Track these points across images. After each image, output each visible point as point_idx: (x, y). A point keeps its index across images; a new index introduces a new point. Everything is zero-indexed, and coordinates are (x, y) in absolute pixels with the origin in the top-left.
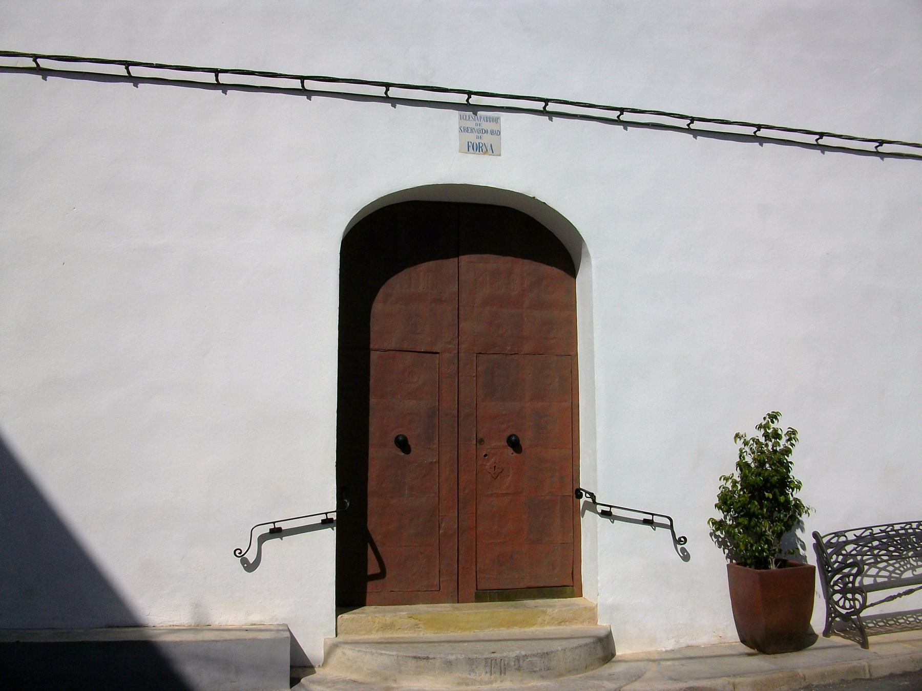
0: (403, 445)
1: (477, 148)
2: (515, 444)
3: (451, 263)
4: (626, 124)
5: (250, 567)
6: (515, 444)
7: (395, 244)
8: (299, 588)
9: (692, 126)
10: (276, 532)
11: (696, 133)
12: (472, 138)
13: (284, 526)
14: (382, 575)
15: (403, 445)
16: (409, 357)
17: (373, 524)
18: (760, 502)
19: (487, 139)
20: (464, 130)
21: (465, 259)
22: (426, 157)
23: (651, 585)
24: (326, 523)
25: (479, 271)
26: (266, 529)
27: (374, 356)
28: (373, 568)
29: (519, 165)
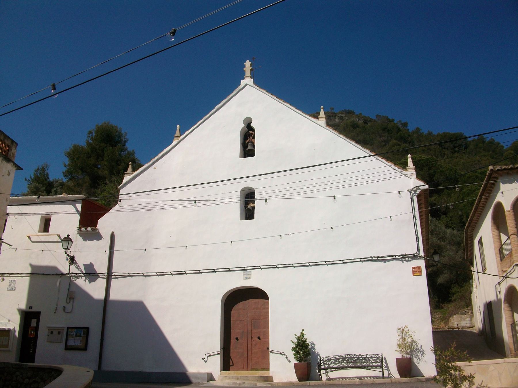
0: (237, 339)
1: (246, 278)
2: (259, 338)
3: (247, 301)
4: (278, 268)
5: (206, 362)
6: (259, 338)
7: (234, 299)
8: (214, 365)
9: (293, 266)
10: (210, 355)
11: (295, 267)
12: (246, 276)
13: (211, 354)
14: (233, 365)
15: (237, 339)
16: (238, 322)
17: (232, 355)
18: (303, 349)
19: (248, 276)
20: (244, 275)
21: (250, 300)
22: (239, 281)
23: (282, 367)
24: (218, 354)
25: (252, 302)
26: (207, 355)
27: (232, 321)
28: (231, 364)
29: (254, 281)
